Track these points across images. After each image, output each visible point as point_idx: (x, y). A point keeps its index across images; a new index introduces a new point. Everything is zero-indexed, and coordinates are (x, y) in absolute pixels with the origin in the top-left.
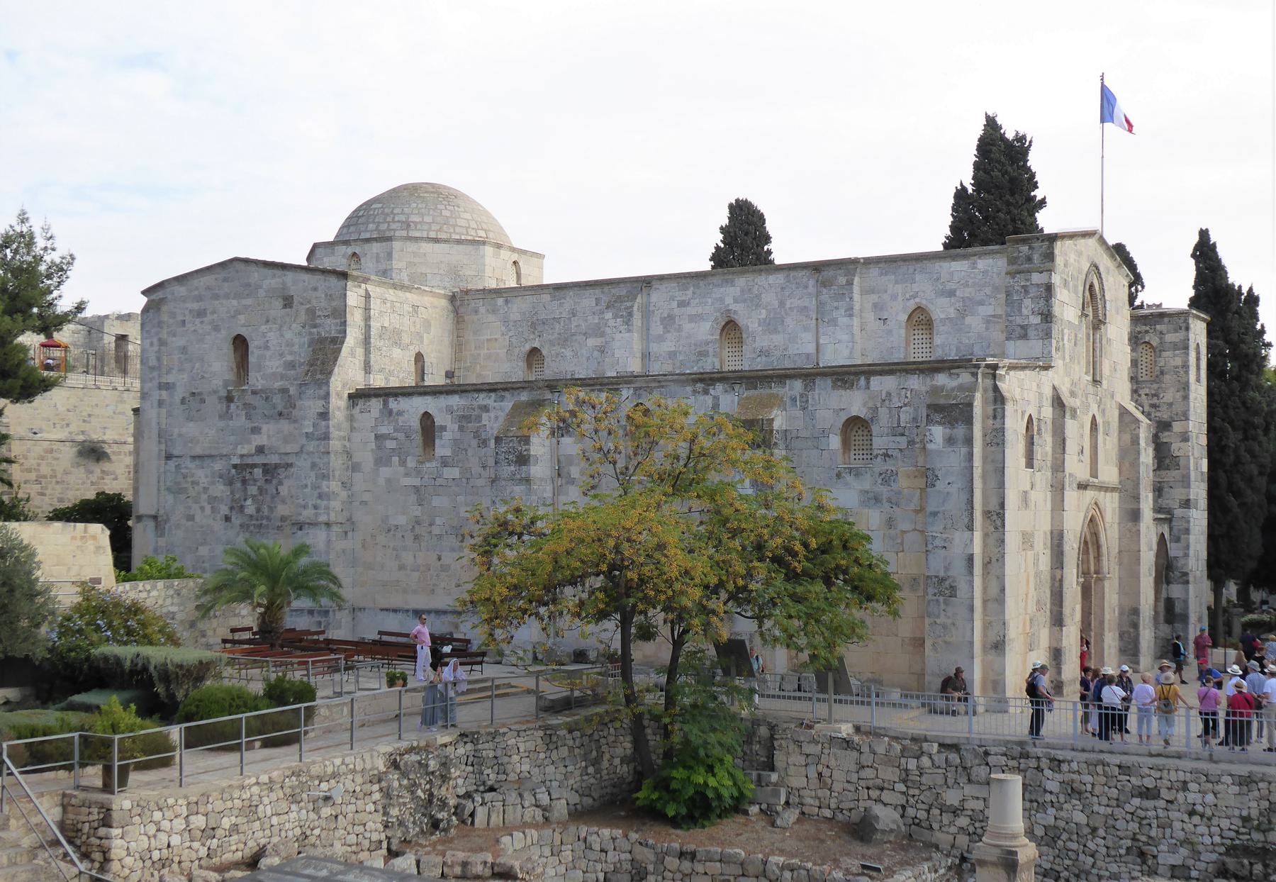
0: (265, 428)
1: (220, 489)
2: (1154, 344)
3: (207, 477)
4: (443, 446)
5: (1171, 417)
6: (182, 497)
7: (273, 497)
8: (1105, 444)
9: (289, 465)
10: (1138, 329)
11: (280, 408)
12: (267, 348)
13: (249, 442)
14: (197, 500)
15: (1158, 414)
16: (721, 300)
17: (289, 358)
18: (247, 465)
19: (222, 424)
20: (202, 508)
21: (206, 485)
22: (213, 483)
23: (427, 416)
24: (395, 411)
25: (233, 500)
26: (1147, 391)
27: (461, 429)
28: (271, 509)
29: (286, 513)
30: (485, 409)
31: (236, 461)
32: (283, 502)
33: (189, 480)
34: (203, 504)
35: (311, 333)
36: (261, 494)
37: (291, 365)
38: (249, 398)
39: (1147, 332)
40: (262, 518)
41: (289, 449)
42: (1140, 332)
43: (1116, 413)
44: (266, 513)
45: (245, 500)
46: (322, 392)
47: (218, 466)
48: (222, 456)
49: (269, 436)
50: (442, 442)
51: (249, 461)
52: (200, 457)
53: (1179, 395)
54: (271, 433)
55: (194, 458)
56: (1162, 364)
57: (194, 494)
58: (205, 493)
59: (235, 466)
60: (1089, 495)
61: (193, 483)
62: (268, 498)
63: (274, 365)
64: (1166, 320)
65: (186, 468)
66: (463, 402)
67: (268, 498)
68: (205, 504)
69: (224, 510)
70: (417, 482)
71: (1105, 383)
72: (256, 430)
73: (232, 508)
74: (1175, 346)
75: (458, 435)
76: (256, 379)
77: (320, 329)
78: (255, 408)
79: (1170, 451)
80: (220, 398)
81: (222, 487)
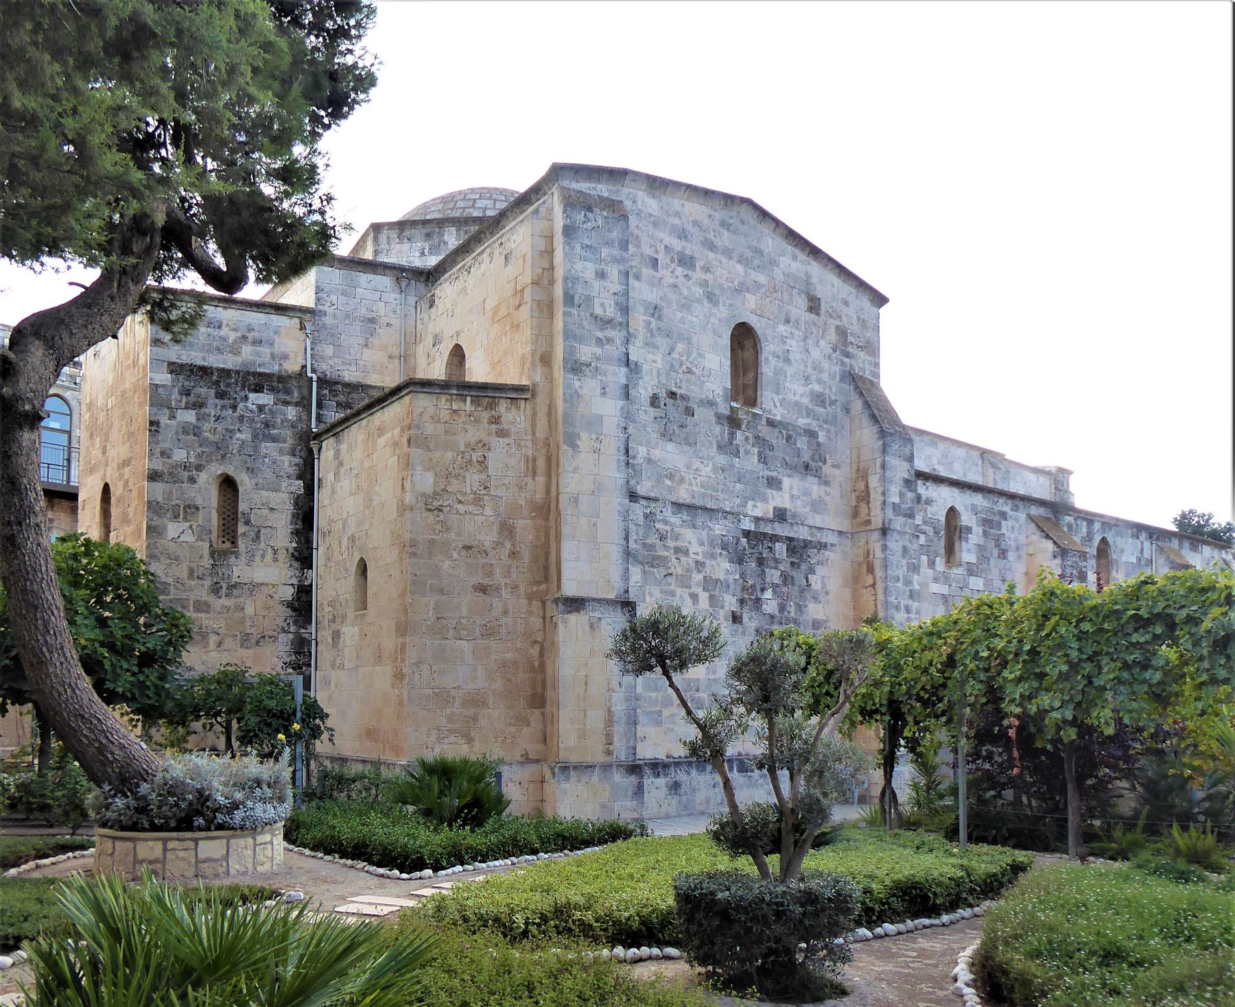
0: (786, 482)
1: (722, 568)
3: (702, 544)
4: (969, 551)
6: (659, 573)
7: (802, 591)
9: (822, 546)
11: (806, 457)
12: (787, 360)
13: (765, 500)
14: (684, 582)
16: (929, 457)
17: (817, 387)
18: (765, 534)
19: (722, 459)
20: (694, 597)
21: (700, 558)
22: (712, 556)
23: (952, 512)
24: (924, 497)
25: (744, 589)
27: (985, 533)
28: (800, 608)
29: (820, 616)
30: (1003, 515)
31: (748, 525)
32: (816, 599)
33: (671, 543)
34: (694, 589)
35: (843, 363)
36: (785, 583)
37: (819, 399)
38: (764, 430)
40: (788, 621)
41: (818, 520)
44: (793, 614)
45: (763, 590)
46: (907, 451)
47: (720, 528)
48: (726, 514)
49: (792, 496)
50: (969, 546)
51: (768, 530)
52: (689, 507)
54: (795, 492)
55: (679, 506)
57: (679, 571)
58: (699, 571)
59: (747, 534)
61: (677, 550)
62: (795, 591)
63: (797, 391)
65: (666, 522)
66: (986, 504)
67: (795, 591)
68: (699, 590)
69: (730, 602)
70: (944, 590)
72: (773, 483)
73: (742, 602)
75: (981, 541)
76: (771, 403)
77: (853, 362)
78: (772, 448)
80: (719, 417)
81: (727, 565)
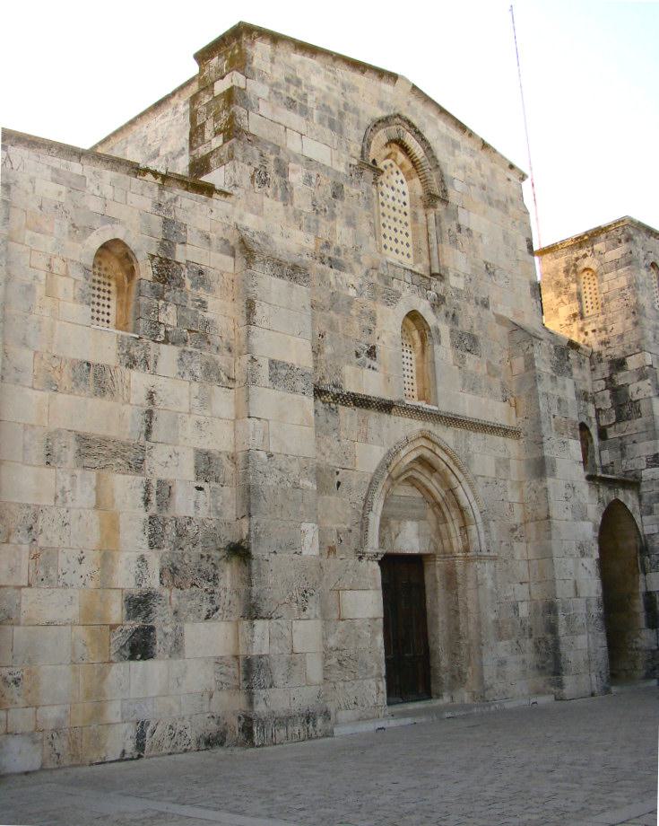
2: (594, 267)
5: (624, 352)
8: (461, 363)
10: (575, 255)
15: (610, 352)
26: (593, 326)
39: (585, 256)
42: (577, 259)
43: (500, 331)
53: (629, 323)
56: (605, 290)
60: (401, 427)
64: (603, 236)
71: (455, 282)
74: (616, 264)
79: (627, 395)
